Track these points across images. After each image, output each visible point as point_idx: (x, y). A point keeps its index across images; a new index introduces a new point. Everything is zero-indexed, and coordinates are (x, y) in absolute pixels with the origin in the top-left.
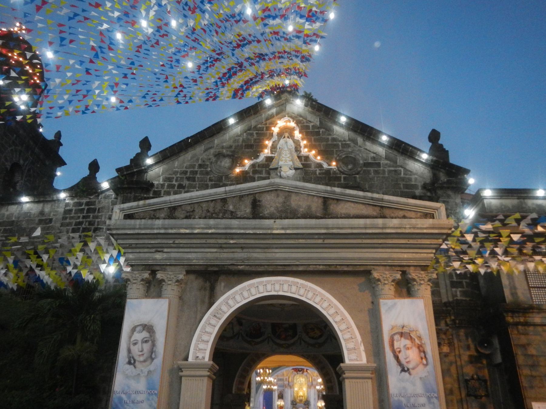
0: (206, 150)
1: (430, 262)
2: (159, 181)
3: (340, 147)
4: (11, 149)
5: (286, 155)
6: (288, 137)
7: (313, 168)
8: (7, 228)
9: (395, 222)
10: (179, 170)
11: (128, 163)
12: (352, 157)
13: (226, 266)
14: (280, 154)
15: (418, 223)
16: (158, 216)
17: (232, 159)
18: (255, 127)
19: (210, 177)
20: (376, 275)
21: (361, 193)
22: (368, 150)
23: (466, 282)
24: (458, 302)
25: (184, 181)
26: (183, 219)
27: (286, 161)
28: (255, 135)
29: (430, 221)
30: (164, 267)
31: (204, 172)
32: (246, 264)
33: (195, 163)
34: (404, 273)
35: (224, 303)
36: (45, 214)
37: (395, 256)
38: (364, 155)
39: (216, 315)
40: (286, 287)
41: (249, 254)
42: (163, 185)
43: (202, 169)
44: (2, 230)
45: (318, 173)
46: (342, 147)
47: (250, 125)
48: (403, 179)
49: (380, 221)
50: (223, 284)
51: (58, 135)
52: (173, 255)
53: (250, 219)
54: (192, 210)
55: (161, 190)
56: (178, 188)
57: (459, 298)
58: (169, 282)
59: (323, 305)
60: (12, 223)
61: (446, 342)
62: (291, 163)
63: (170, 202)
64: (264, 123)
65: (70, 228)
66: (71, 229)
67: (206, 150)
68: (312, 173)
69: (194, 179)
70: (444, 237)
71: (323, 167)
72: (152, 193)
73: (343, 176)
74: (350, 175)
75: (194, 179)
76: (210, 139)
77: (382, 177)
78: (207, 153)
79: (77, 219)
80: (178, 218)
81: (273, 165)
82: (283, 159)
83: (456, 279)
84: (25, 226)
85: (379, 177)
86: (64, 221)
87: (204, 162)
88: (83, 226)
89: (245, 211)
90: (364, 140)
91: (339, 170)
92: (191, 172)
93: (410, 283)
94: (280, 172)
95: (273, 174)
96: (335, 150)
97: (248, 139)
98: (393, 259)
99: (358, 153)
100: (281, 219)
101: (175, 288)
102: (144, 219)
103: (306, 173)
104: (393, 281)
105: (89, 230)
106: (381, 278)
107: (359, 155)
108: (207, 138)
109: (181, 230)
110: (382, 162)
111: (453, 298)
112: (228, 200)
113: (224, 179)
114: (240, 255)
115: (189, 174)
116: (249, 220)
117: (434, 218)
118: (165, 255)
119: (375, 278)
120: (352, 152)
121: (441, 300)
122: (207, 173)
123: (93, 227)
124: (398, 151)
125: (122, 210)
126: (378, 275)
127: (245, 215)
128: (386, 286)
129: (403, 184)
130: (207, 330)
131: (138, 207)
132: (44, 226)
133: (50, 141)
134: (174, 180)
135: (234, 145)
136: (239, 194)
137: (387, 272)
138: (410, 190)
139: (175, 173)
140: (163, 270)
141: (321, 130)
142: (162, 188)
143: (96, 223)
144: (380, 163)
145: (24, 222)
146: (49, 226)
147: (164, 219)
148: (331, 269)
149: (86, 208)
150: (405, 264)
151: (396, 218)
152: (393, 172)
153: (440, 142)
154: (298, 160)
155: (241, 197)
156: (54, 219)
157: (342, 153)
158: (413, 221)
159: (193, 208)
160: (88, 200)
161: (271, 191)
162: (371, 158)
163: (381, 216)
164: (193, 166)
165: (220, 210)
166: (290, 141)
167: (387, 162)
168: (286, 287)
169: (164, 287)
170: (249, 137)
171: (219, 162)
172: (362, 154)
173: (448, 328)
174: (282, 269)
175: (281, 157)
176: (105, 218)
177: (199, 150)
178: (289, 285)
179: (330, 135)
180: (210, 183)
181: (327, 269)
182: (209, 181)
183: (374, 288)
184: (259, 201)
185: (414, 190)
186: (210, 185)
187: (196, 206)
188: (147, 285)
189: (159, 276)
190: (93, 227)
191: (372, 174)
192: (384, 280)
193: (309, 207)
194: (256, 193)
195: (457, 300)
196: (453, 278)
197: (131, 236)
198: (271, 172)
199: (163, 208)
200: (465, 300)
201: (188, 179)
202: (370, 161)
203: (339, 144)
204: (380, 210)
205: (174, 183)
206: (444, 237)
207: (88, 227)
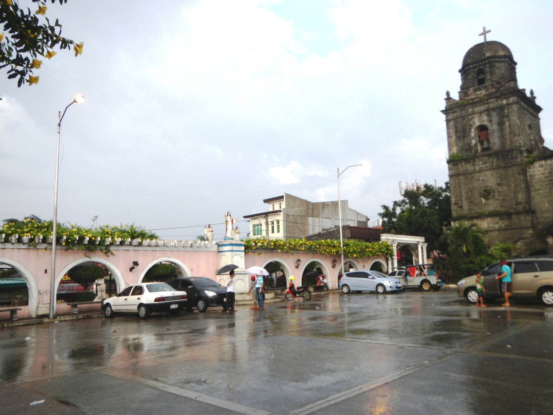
51: (532, 93)
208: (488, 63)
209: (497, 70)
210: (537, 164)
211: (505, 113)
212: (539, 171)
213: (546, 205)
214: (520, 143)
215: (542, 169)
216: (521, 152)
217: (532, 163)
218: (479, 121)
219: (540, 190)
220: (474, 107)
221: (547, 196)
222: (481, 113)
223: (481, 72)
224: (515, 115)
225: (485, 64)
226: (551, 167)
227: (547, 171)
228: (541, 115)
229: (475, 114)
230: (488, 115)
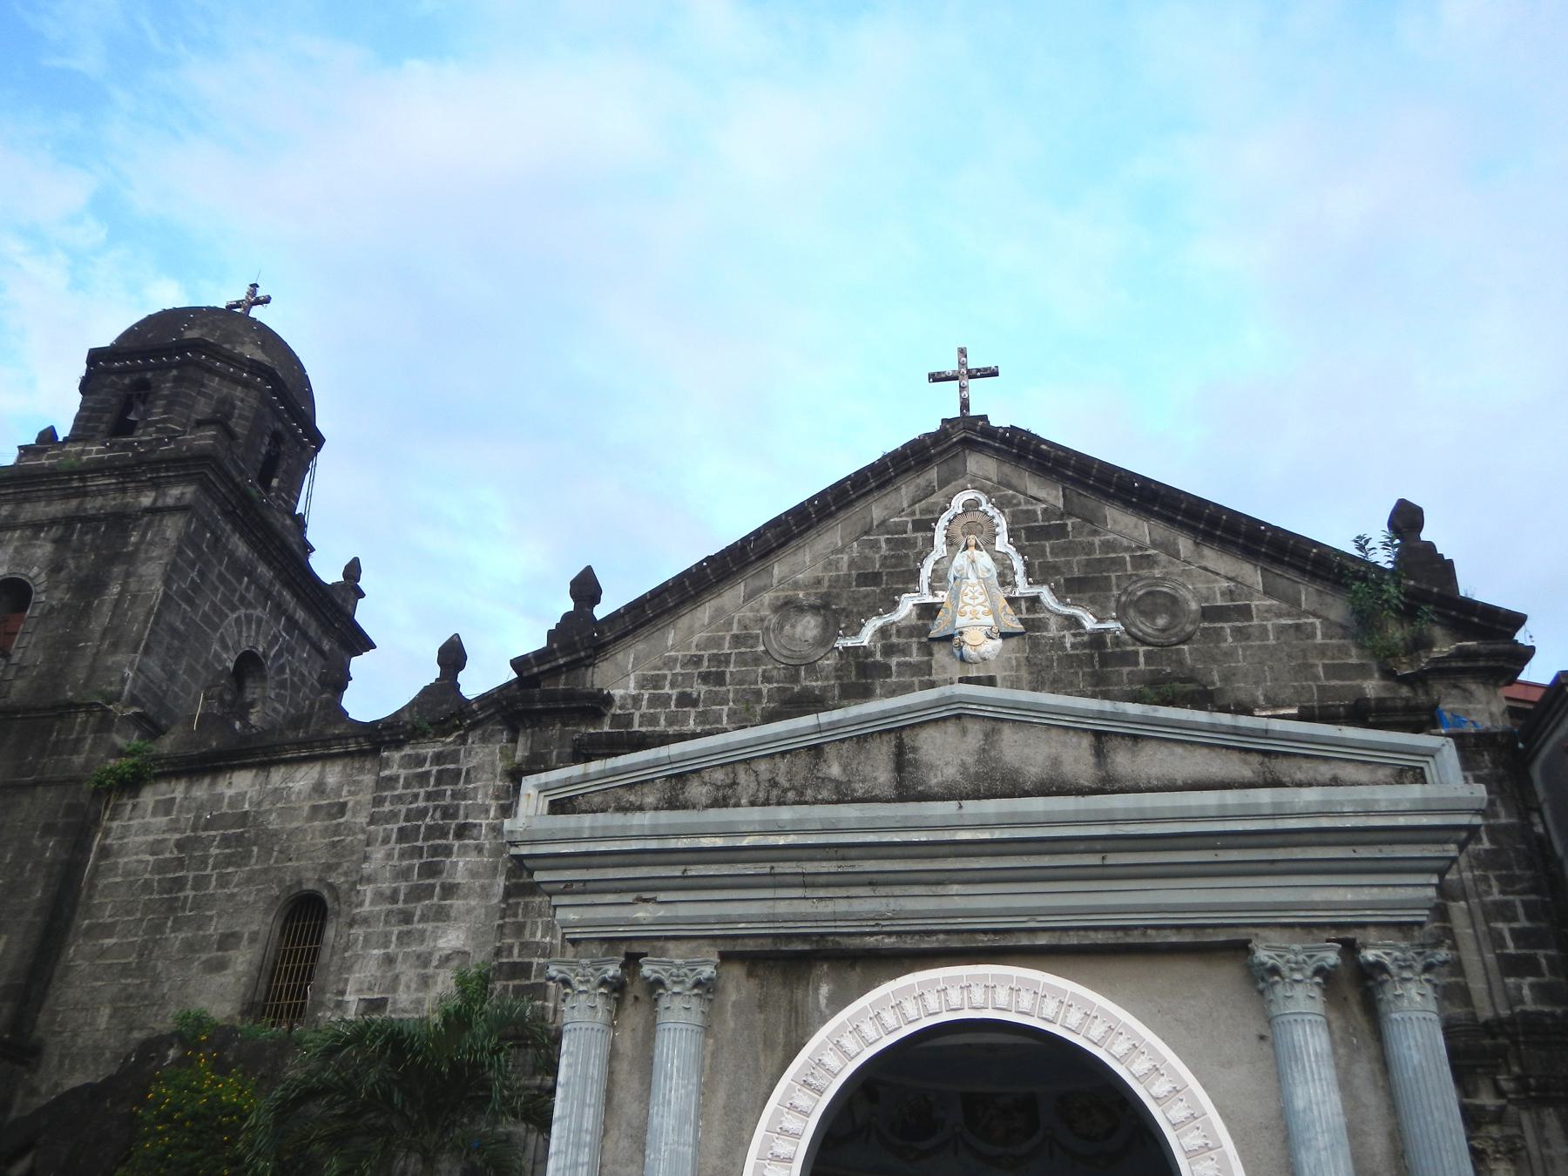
0: (749, 597)
1: (1427, 912)
2: (627, 688)
3: (1129, 567)
4: (235, 616)
5: (973, 598)
6: (977, 547)
8: (231, 832)
9: (1310, 796)
10: (680, 654)
11: (542, 643)
12: (1166, 594)
13: (831, 938)
14: (956, 596)
15: (1377, 797)
16: (638, 803)
17: (825, 616)
18: (883, 523)
19: (764, 671)
20: (1263, 955)
21: (1201, 716)
22: (1212, 572)
23: (1547, 957)
24: (1531, 1023)
25: (695, 686)
26: (707, 807)
27: (975, 616)
28: (883, 545)
29: (1414, 791)
30: (660, 944)
31: (748, 657)
32: (885, 929)
33: (721, 634)
34: (1350, 948)
35: (831, 1046)
36: (328, 790)
37: (1318, 896)
38: (1201, 586)
39: (811, 1080)
40: (1002, 997)
41: (892, 900)
42: (636, 700)
43: (743, 650)
44: (218, 839)
45: (1068, 645)
46: (1135, 567)
47: (868, 520)
49: (1265, 796)
50: (824, 990)
51: (353, 570)
52: (683, 911)
53: (888, 801)
54: (728, 781)
55: (632, 714)
56: (676, 706)
57: (1530, 1007)
58: (677, 989)
59: (1115, 1047)
61: (1501, 1149)
62: (990, 620)
63: (671, 763)
65: (395, 827)
66: (395, 830)
67: (749, 597)
68: (1052, 645)
69: (719, 679)
70: (1464, 835)
71: (1084, 628)
72: (607, 720)
73: (1142, 649)
74: (1162, 646)
75: (719, 679)
76: (759, 566)
77: (1260, 647)
79: (411, 803)
80: (694, 808)
81: (938, 628)
82: (967, 609)
83: (1517, 947)
84: (275, 827)
85: (1251, 646)
86: (377, 809)
87: (746, 628)
88: (428, 820)
89: (875, 778)
90: (1197, 544)
91: (1128, 632)
93: (1371, 977)
94: (960, 648)
95: (940, 655)
96: (1113, 576)
97: (866, 558)
98: (1313, 906)
99: (1181, 579)
100: (978, 798)
101: (695, 1003)
102: (603, 811)
103: (1035, 645)
104: (1319, 971)
105: (444, 835)
106: (1280, 963)
107: (1184, 586)
108: (752, 562)
109: (702, 840)
110: (1254, 604)
111: (1511, 1007)
112: (827, 748)
113: (803, 673)
114: (868, 904)
115: (706, 663)
116: (888, 805)
117: (1425, 782)
118: (662, 912)
119: (1263, 964)
120: (1163, 579)
121: (1474, 1017)
122: (757, 660)
123: (453, 824)
124: (1303, 572)
126: (1272, 954)
127: (877, 792)
128: (1299, 989)
129: (1325, 666)
130: (786, 1125)
131: (585, 778)
132: (326, 823)
133: (334, 585)
134: (667, 683)
135: (827, 575)
136: (855, 731)
137: (1297, 947)
138: (1348, 683)
139: (670, 663)
140: (659, 952)
141: (1069, 522)
142: (633, 708)
143: (462, 812)
144: (1249, 606)
145: (274, 815)
146: (340, 824)
147: (656, 809)
148: (1130, 940)
149: (435, 769)
150: (1349, 920)
151: (1310, 785)
152: (1292, 631)
153: (1425, 535)
154: (1009, 609)
155: (862, 739)
156: (350, 805)
157: (1135, 582)
158: (1362, 793)
159: (731, 776)
160: (438, 748)
161: (944, 719)
162: (1223, 594)
163: (1265, 779)
164: (717, 642)
165: (806, 779)
166: (984, 559)
167: (1268, 602)
168: (1002, 997)
169: (664, 1002)
171: (787, 627)
172: (1193, 584)
173: (1502, 1102)
174: (989, 944)
175: (961, 605)
176: (486, 795)
177: (731, 597)
178: (1011, 989)
179: (1095, 533)
180: (765, 688)
181: (1120, 941)
182: (762, 683)
183: (1261, 992)
184: (914, 750)
185: (1358, 682)
186: (765, 691)
187: (741, 769)
188: (616, 995)
189: (646, 970)
190: (453, 824)
191: (1230, 639)
192: (1292, 970)
193: (1056, 762)
194: (903, 728)
195: (1525, 1013)
196: (1503, 946)
197: (571, 861)
198: (936, 648)
199: (653, 780)
200: (1552, 1015)
201: (705, 678)
202: (1219, 602)
203: (1124, 558)
204: (1262, 764)
205: (667, 690)
206: (1464, 835)
207: (441, 822)
208: (178, 365)
209: (203, 400)
210: (149, 797)
211: (126, 544)
212: (146, 830)
213: (103, 1017)
214: (123, 681)
215: (162, 821)
216: (106, 723)
217: (131, 784)
218: (13, 559)
219: (108, 930)
220: (27, 500)
221: (125, 970)
222: (36, 527)
223: (142, 391)
224: (160, 558)
225: (170, 367)
226: (198, 817)
227: (177, 836)
228: (358, 664)
229: (14, 528)
230: (61, 542)
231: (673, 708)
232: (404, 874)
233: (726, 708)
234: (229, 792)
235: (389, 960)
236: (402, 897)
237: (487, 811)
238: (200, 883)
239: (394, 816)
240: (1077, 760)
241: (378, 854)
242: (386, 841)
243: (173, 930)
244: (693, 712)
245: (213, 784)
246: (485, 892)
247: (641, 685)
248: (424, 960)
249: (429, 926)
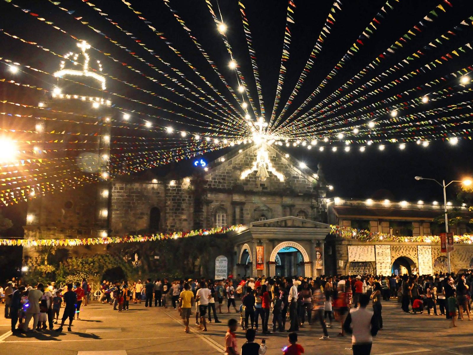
7: (273, 177)
18: (249, 155)
48: (307, 185)
60: (139, 192)
64: (253, 152)
65: (171, 198)
72: (207, 184)
78: (229, 166)
92: (223, 175)
125: (252, 224)
139: (216, 175)
164: (223, 173)
167: (301, 176)
170: (247, 160)
171: (235, 172)
179: (280, 161)
202: (295, 176)
205: (216, 180)
227: (126, 194)
231: (218, 183)
232: (174, 206)
233: (226, 184)
234: (135, 187)
235: (174, 219)
236: (174, 210)
237: (187, 197)
238: (134, 203)
239: (170, 196)
240: (301, 225)
241: (169, 203)
242: (170, 200)
243: (130, 211)
244: (221, 185)
245: (131, 185)
246: (188, 210)
247: (213, 178)
248: (180, 220)
249: (180, 215)
